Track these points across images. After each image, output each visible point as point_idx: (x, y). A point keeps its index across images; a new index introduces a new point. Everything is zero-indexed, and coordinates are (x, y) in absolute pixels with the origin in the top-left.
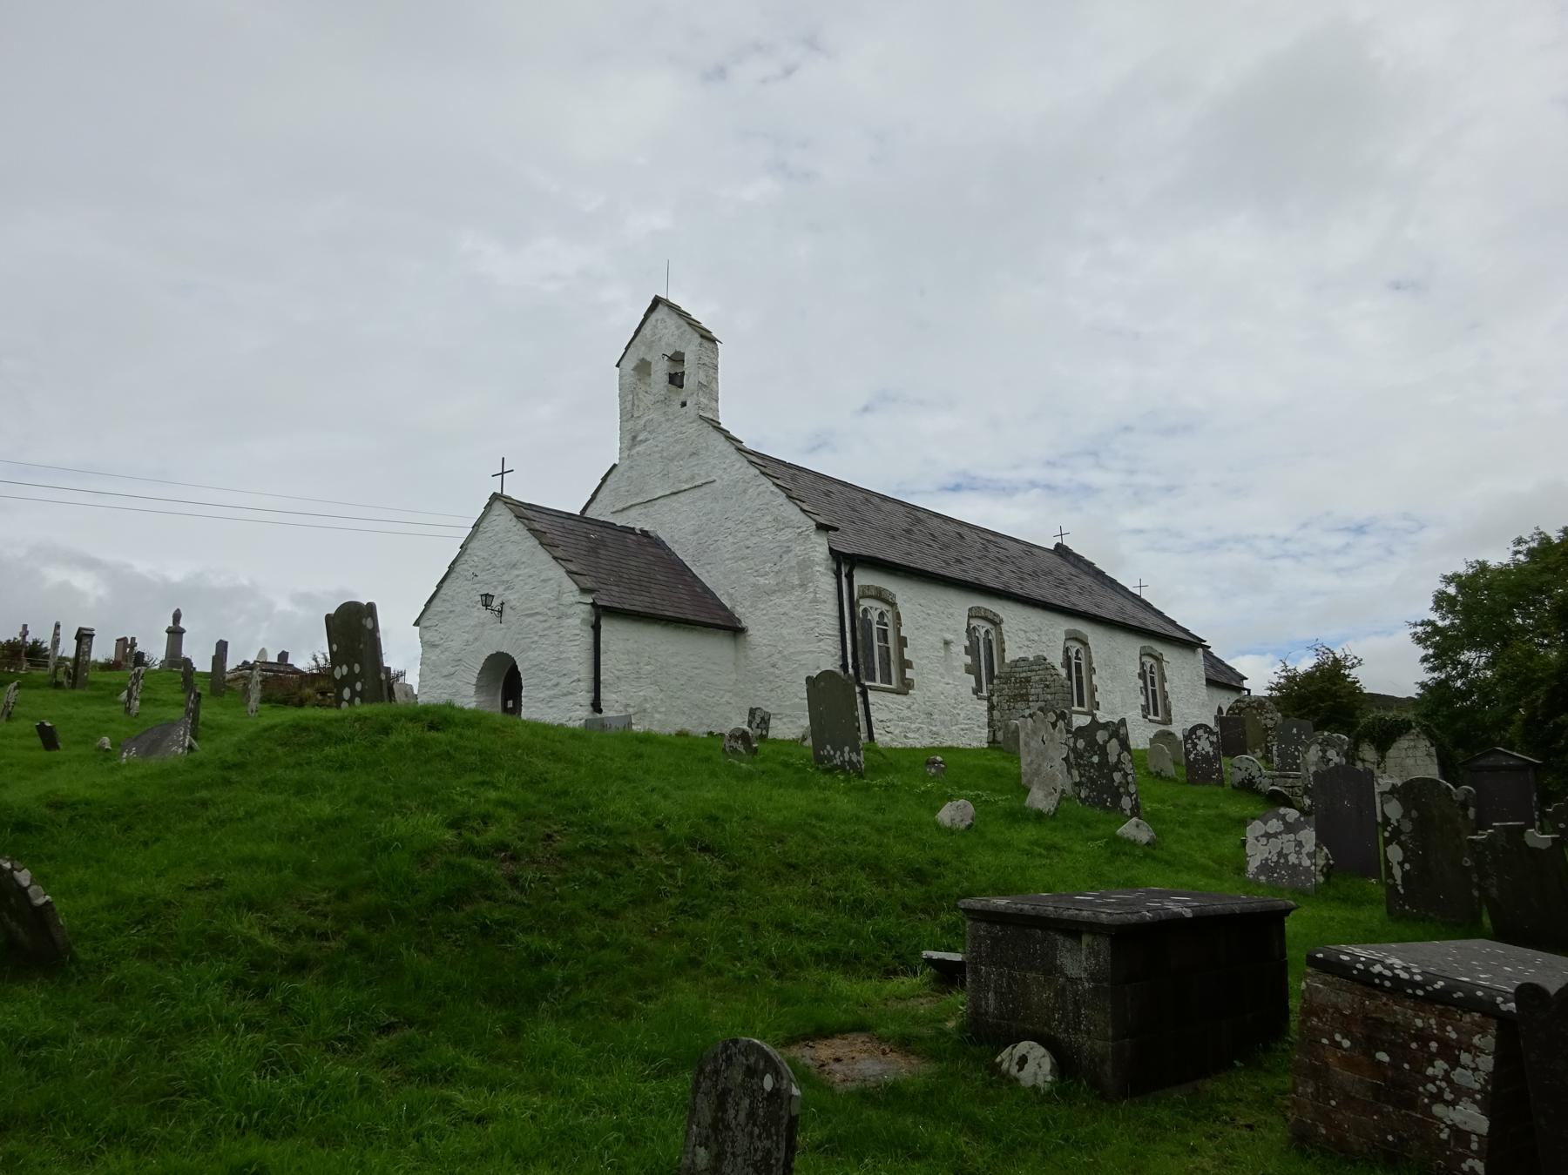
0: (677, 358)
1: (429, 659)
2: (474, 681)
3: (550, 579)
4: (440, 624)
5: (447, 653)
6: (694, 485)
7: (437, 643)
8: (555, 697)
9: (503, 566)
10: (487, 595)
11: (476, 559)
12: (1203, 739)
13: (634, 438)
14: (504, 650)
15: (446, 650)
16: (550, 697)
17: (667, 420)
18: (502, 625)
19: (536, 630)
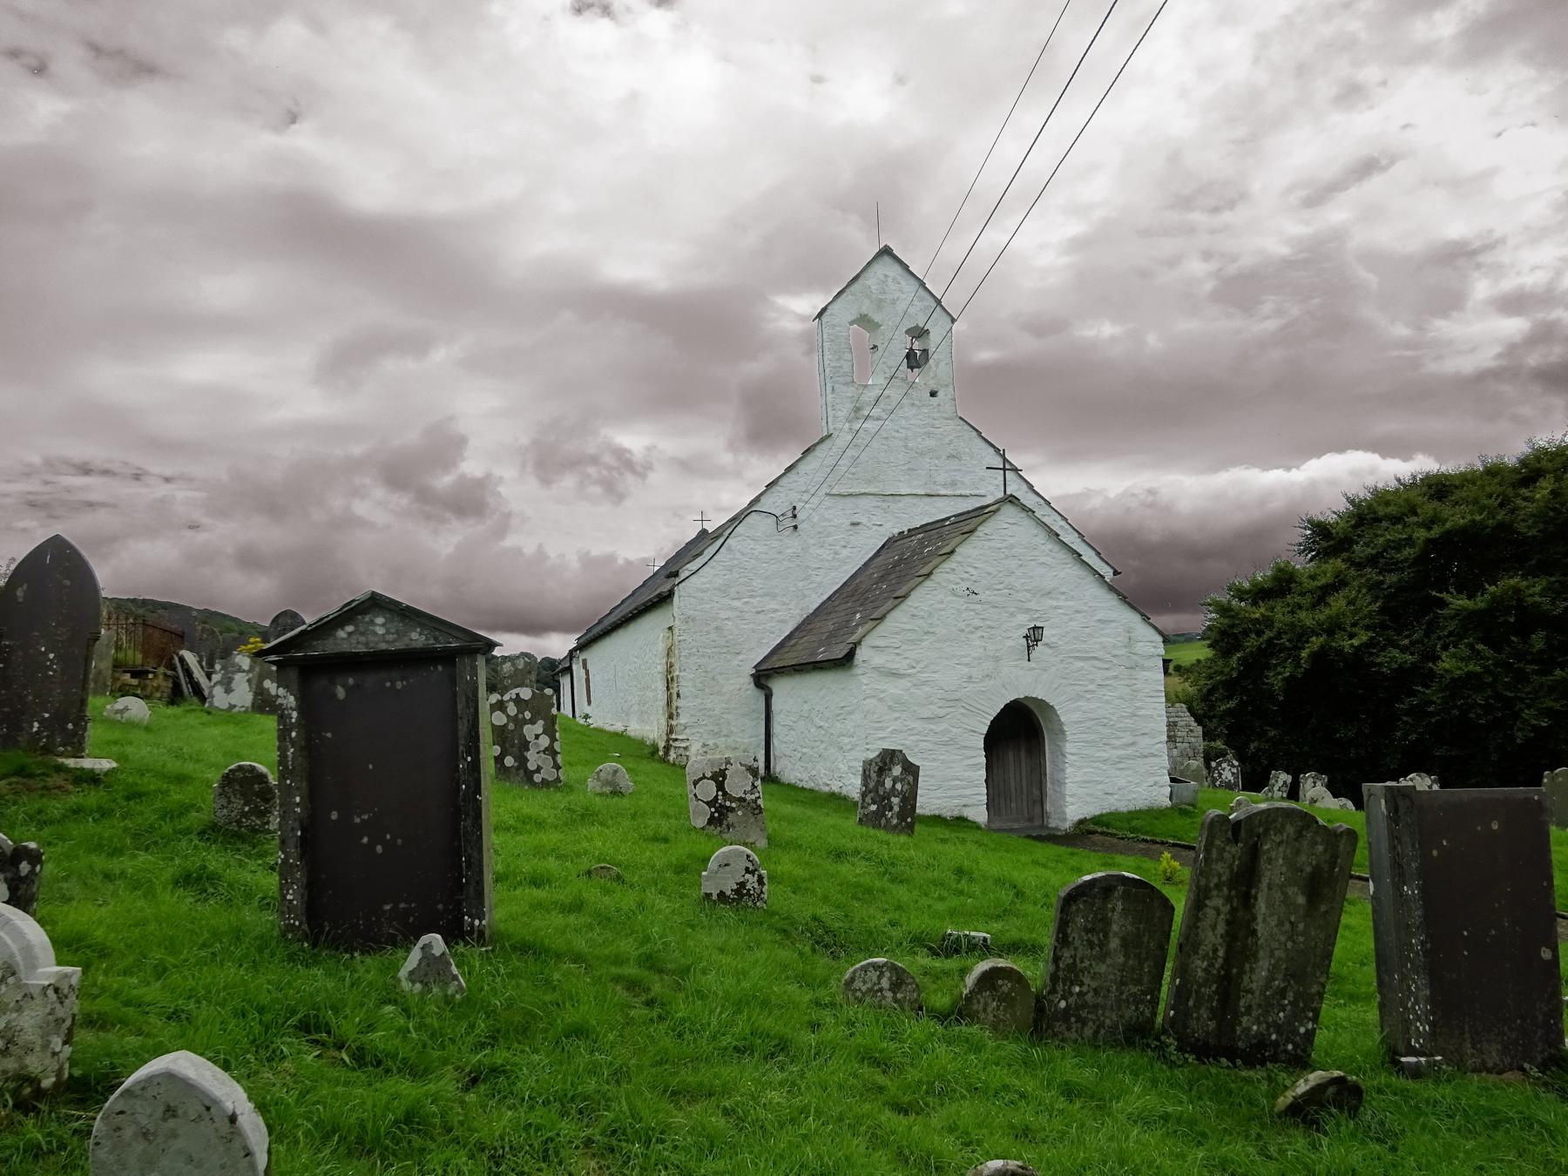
0: (919, 333)
1: (883, 692)
2: (985, 730)
3: (1112, 621)
4: (903, 647)
5: (927, 689)
6: (958, 492)
7: (902, 672)
8: (1128, 757)
9: (1028, 591)
10: (1035, 628)
11: (970, 569)
12: (1227, 770)
13: (857, 410)
14: (1038, 693)
15: (924, 683)
16: (1118, 757)
17: (913, 405)
18: (1032, 664)
19: (1090, 677)
